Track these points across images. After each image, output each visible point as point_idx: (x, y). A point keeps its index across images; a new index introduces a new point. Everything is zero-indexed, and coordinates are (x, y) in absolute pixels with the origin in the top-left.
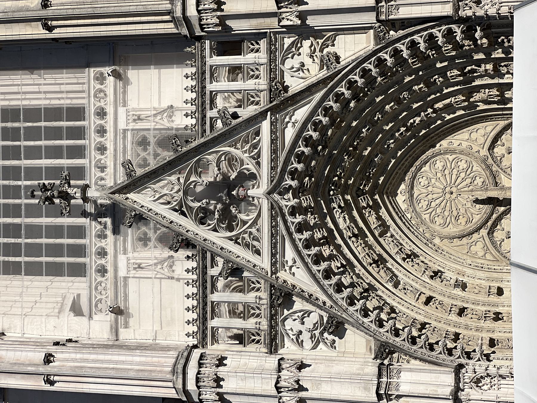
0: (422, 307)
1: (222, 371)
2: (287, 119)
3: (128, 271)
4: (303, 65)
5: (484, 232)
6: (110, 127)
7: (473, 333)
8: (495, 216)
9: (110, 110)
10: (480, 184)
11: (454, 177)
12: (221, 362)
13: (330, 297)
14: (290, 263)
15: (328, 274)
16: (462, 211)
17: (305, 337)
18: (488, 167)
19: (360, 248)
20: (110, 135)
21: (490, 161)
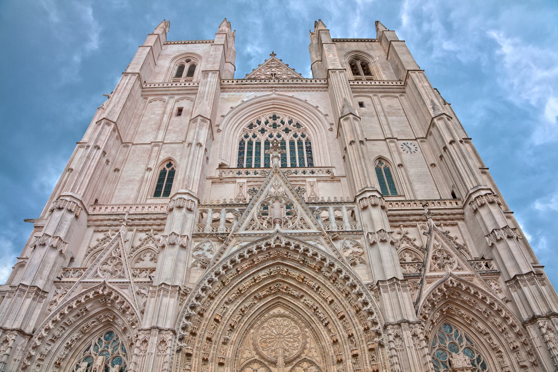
0: (213, 317)
1: (184, 210)
2: (318, 241)
3: (238, 183)
4: (348, 248)
5: (257, 357)
7: (196, 345)
8: (266, 363)
9: (314, 175)
10: (285, 355)
11: (289, 340)
12: (190, 210)
13: (221, 263)
14: (241, 244)
15: (232, 262)
16: (269, 345)
17: (200, 252)
18: (295, 359)
19: (248, 283)
21: (299, 360)
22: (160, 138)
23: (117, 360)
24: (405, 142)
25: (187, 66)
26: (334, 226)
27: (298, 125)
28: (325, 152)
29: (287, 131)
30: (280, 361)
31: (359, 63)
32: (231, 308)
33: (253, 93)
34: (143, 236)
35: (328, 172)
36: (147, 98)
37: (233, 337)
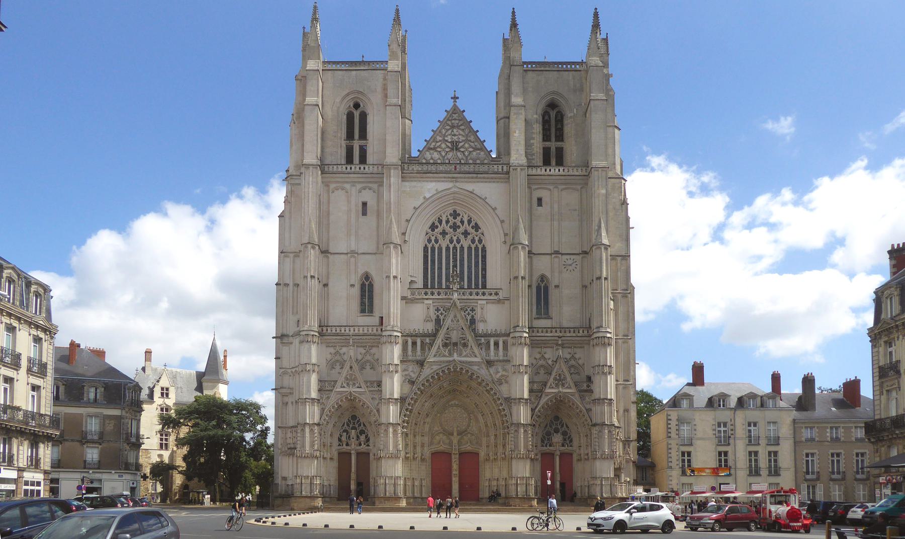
6: (479, 297)
9: (485, 297)
15: (428, 381)
17: (407, 373)
20: (476, 297)
22: (353, 247)
23: (362, 432)
24: (568, 257)
25: (357, 114)
26: (492, 355)
27: (477, 227)
28: (495, 275)
29: (466, 234)
30: (455, 434)
31: (553, 114)
32: (427, 404)
33: (433, 184)
34: (362, 350)
35: (497, 294)
36: (328, 186)
37: (428, 420)
